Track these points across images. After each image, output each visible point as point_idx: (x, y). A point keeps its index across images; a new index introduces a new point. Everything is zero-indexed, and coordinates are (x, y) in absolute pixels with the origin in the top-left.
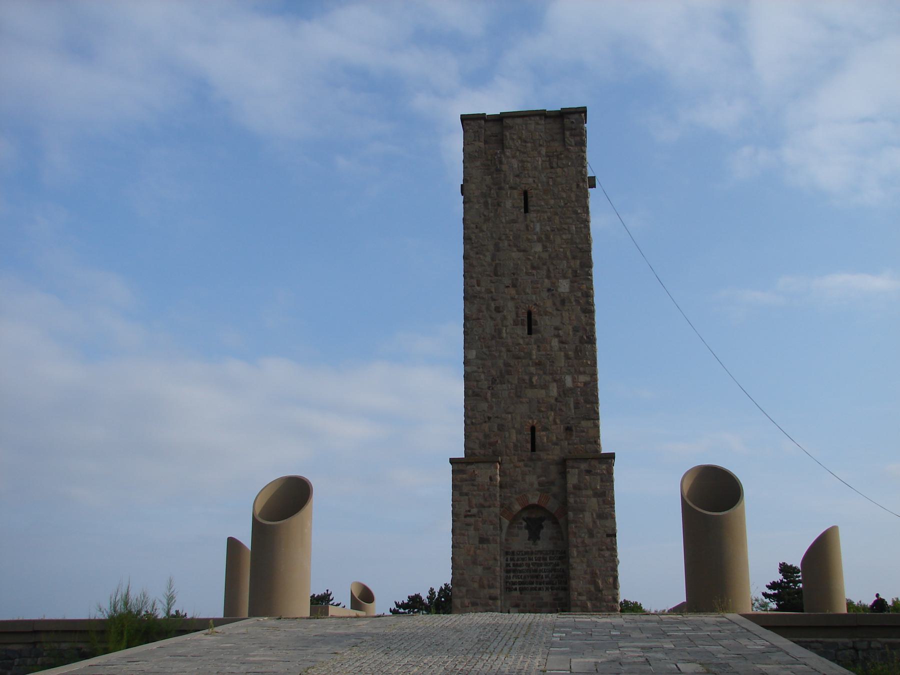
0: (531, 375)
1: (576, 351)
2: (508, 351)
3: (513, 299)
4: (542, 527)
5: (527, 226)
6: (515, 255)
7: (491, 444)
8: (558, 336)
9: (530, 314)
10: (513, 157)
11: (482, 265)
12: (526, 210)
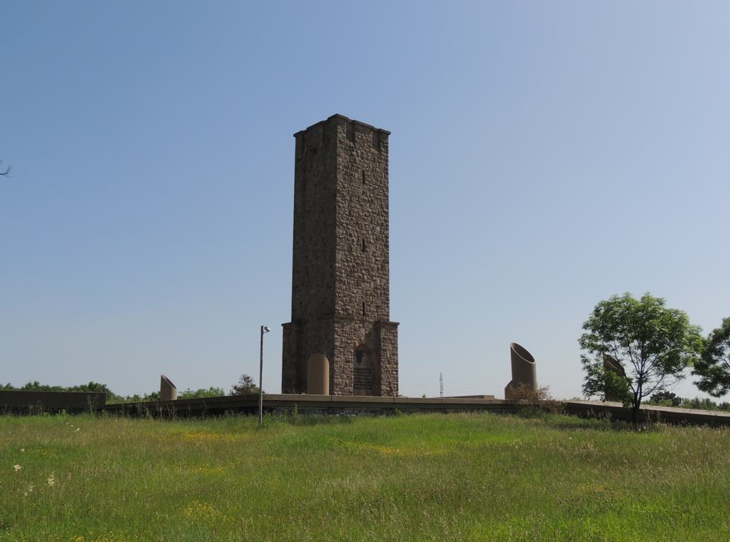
0: (363, 275)
1: (382, 266)
2: (355, 259)
3: (357, 231)
4: (362, 356)
5: (364, 192)
6: (358, 206)
7: (347, 310)
8: (375, 257)
9: (364, 241)
10: (359, 149)
11: (344, 208)
12: (364, 183)
